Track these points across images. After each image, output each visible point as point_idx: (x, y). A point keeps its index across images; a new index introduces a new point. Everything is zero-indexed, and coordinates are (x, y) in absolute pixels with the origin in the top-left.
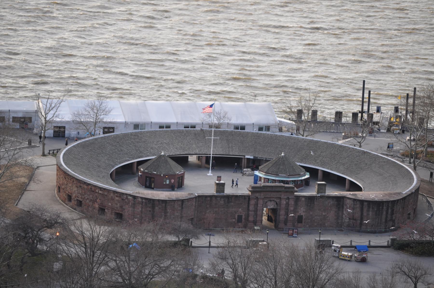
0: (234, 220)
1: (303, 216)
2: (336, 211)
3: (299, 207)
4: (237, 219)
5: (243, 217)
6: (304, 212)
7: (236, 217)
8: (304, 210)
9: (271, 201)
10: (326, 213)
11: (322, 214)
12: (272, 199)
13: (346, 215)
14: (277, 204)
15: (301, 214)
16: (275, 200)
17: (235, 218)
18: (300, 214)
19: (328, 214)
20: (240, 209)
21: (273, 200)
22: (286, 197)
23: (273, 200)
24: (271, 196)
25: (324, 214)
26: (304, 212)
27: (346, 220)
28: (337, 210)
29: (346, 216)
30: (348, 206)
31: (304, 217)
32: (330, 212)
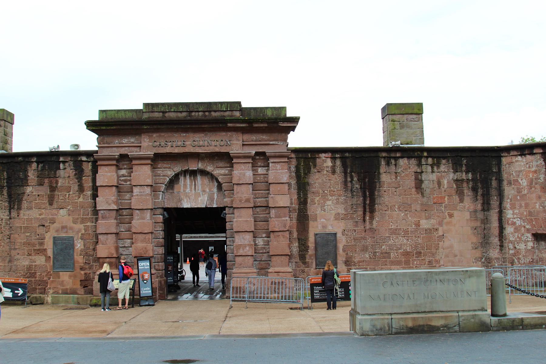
0: (40, 260)
1: (339, 235)
2: (475, 211)
3: (317, 198)
4: (50, 253)
5: (79, 245)
6: (337, 217)
7: (49, 245)
8: (341, 210)
9: (193, 173)
10: (433, 221)
11: (418, 225)
12: (193, 166)
13: (518, 223)
14: (220, 187)
15: (330, 229)
16: (209, 168)
17: (42, 251)
18: (324, 227)
19: (440, 224)
20: (62, 212)
21: (204, 173)
22: (253, 151)
23: (204, 173)
24: (187, 150)
25: (425, 224)
26: (337, 217)
27: (522, 246)
28: (479, 207)
29: (517, 230)
30: (524, 183)
31: (342, 242)
32: (451, 216)
